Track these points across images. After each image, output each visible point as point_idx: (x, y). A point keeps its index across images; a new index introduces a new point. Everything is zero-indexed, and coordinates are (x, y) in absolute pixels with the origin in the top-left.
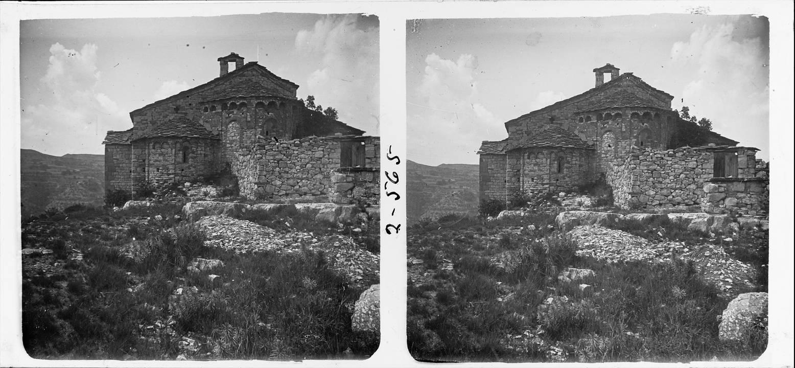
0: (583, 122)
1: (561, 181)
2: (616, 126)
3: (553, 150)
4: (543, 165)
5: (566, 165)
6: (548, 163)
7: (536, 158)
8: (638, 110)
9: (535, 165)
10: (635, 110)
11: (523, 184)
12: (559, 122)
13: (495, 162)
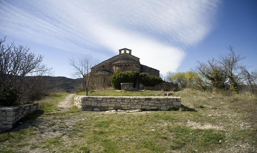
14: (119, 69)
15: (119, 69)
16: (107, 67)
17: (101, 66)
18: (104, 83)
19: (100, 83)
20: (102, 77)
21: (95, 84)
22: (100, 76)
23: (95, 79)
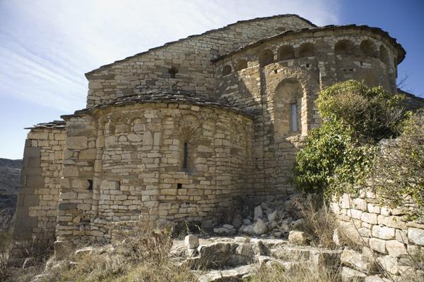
1: (188, 189)
3: (170, 112)
4: (143, 149)
5: (201, 148)
6: (157, 142)
7: (130, 132)
8: (350, 35)
9: (124, 148)
10: (345, 35)
11: (99, 194)
12: (185, 75)
14: (297, 74)
15: (297, 74)
16: (198, 77)
17: (158, 67)
18: (183, 177)
19: (149, 178)
20: (170, 123)
22: (150, 114)
23: (111, 140)
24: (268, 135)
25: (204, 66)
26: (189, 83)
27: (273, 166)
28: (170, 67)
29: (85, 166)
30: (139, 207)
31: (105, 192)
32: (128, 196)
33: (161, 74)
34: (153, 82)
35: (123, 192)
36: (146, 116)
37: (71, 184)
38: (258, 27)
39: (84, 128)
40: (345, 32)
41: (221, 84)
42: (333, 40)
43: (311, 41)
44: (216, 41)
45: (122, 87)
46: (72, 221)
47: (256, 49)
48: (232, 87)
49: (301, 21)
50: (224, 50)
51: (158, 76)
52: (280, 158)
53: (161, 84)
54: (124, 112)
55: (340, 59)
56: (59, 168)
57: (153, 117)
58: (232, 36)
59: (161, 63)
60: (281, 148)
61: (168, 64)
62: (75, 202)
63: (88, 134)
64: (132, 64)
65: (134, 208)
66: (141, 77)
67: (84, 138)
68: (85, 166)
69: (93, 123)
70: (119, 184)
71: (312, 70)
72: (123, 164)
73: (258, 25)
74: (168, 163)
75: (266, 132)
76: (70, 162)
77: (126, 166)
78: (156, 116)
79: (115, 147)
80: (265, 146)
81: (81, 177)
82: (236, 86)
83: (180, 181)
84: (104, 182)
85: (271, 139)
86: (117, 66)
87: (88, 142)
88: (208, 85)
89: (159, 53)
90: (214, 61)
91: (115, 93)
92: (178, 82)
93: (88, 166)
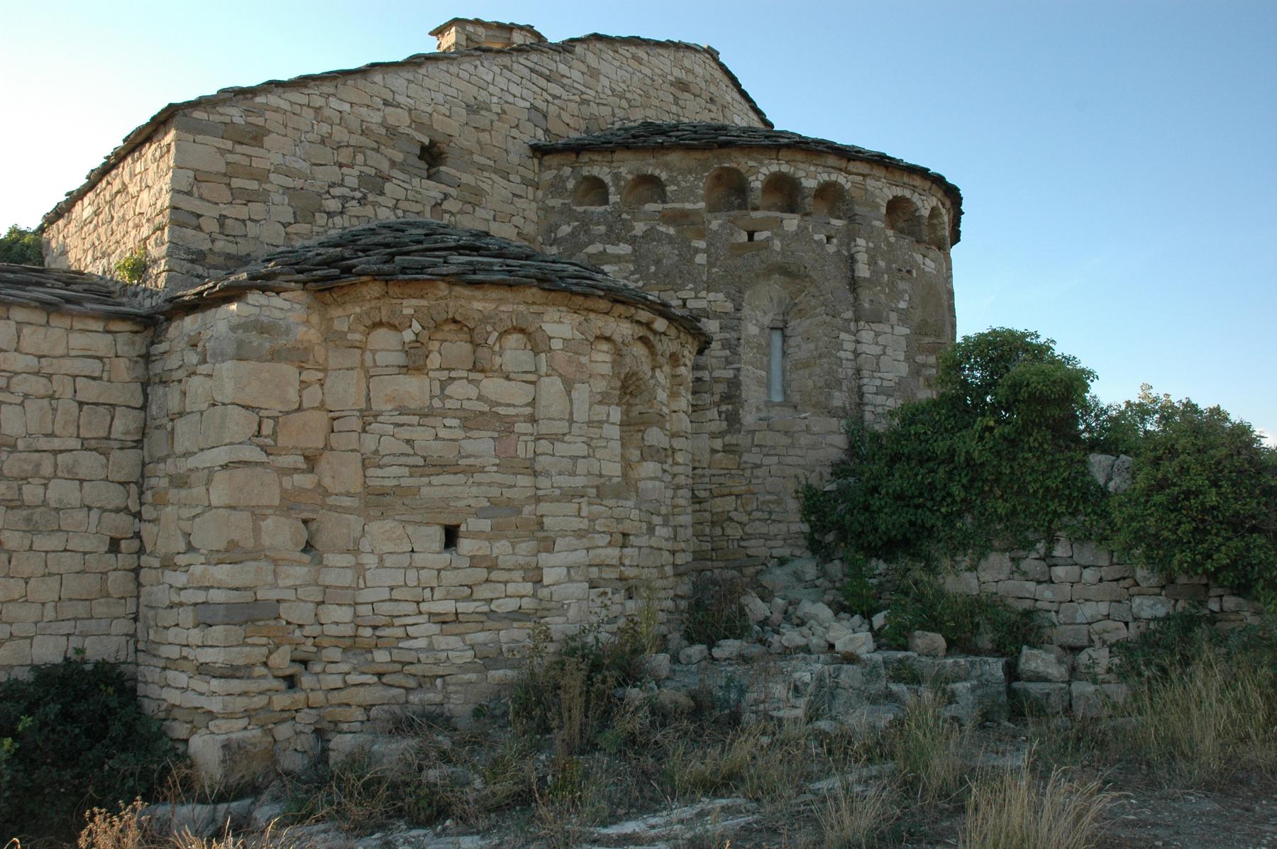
0: (606, 202)
2: (819, 243)
4: (544, 428)
9: (470, 421)
10: (904, 185)
12: (466, 178)
13: (38, 386)
16: (497, 190)
17: (392, 131)
21: (383, 534)
24: (724, 408)
25: (514, 158)
26: (474, 205)
27: (736, 490)
28: (426, 141)
29: (296, 470)
30: (527, 604)
31: (389, 561)
32: (490, 569)
33: (399, 157)
34: (375, 183)
35: (472, 558)
36: (549, 328)
37: (257, 531)
38: (635, 64)
39: (288, 331)
40: (906, 179)
41: (565, 230)
42: (884, 190)
43: (841, 179)
44: (542, 82)
45: (289, 182)
46: (265, 664)
47: (698, 155)
48: (611, 249)
49: (719, 74)
50: (559, 116)
51: (393, 164)
52: (758, 472)
53: (401, 194)
54: (477, 305)
55: (892, 240)
56: (47, 470)
57: (568, 335)
58: (576, 75)
59: (398, 118)
60: (760, 446)
61: (419, 125)
62: (273, 595)
63: (299, 356)
64: (318, 102)
65: (512, 604)
66: (344, 156)
67: (289, 370)
68: (296, 470)
69: (315, 319)
70: (451, 536)
71: (838, 252)
72: (470, 471)
73: (634, 57)
74: (601, 476)
75: (717, 398)
76: (255, 454)
77: (478, 477)
78: (578, 335)
79: (425, 414)
80: (713, 436)
81: (288, 505)
82: (624, 249)
83: (626, 526)
84: (374, 527)
85: (733, 420)
86: (273, 100)
87: (304, 384)
88: (518, 220)
89: (398, 81)
90: (539, 151)
91: (263, 197)
92: (446, 196)
93: (303, 472)
